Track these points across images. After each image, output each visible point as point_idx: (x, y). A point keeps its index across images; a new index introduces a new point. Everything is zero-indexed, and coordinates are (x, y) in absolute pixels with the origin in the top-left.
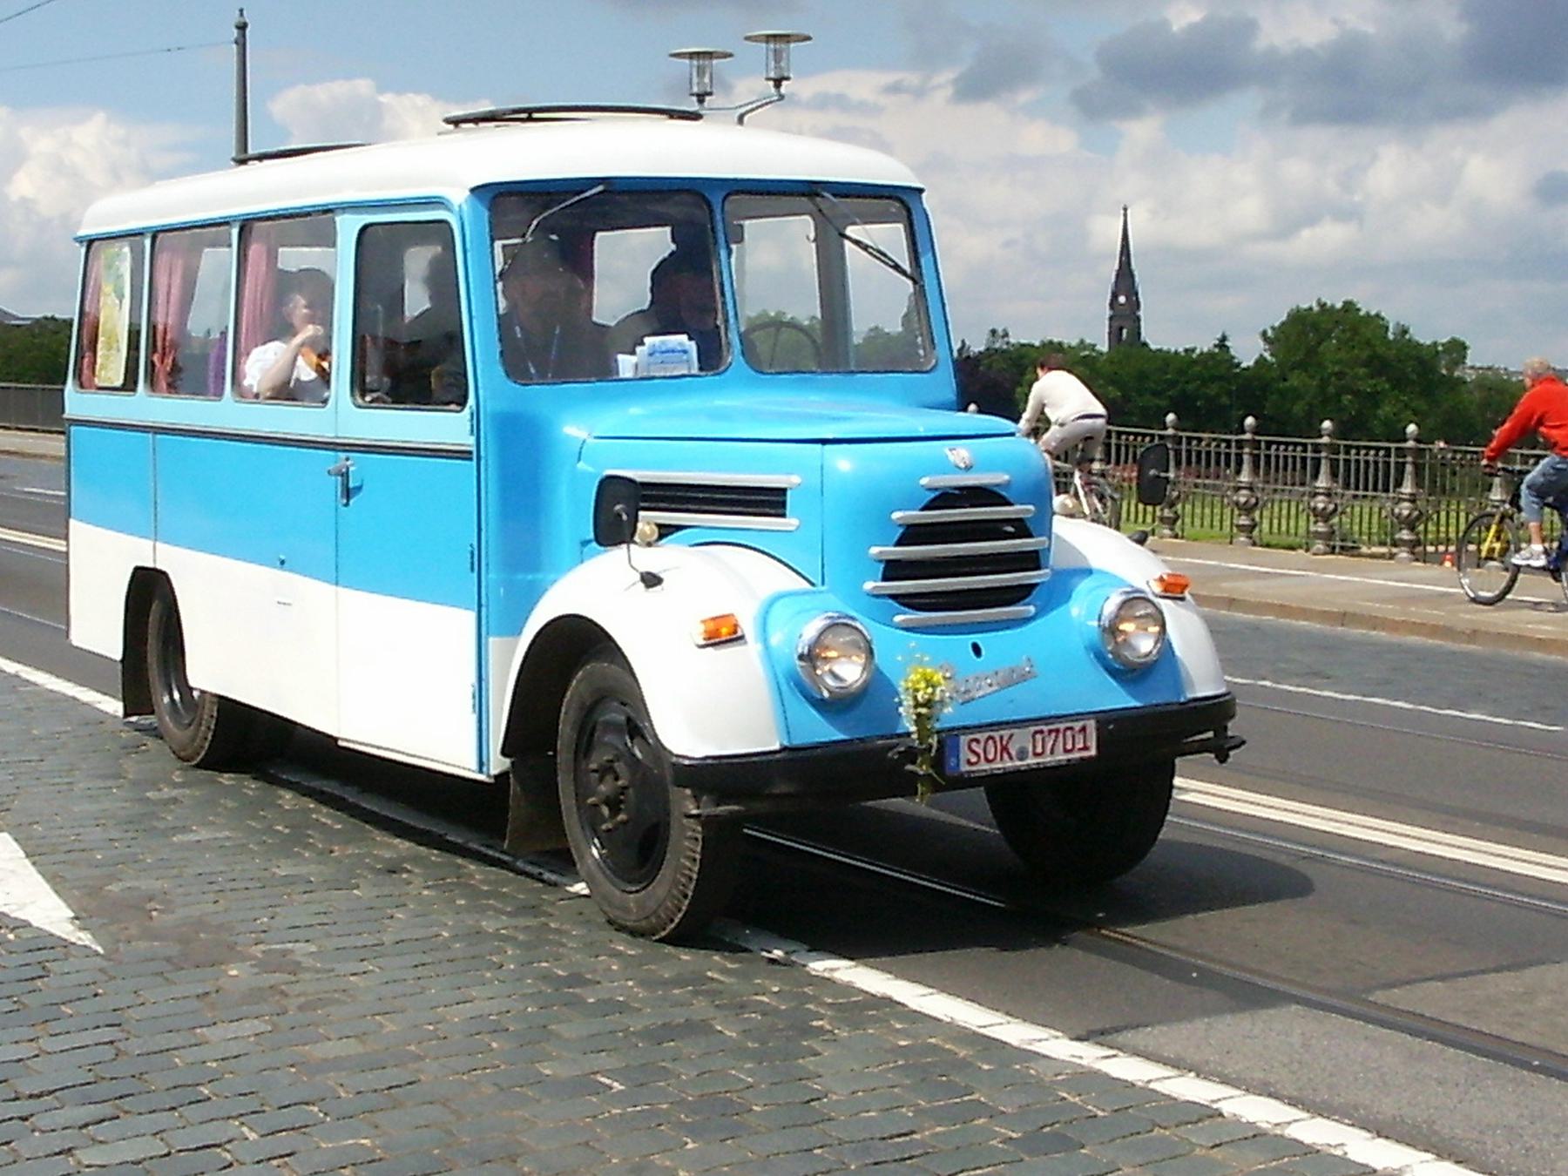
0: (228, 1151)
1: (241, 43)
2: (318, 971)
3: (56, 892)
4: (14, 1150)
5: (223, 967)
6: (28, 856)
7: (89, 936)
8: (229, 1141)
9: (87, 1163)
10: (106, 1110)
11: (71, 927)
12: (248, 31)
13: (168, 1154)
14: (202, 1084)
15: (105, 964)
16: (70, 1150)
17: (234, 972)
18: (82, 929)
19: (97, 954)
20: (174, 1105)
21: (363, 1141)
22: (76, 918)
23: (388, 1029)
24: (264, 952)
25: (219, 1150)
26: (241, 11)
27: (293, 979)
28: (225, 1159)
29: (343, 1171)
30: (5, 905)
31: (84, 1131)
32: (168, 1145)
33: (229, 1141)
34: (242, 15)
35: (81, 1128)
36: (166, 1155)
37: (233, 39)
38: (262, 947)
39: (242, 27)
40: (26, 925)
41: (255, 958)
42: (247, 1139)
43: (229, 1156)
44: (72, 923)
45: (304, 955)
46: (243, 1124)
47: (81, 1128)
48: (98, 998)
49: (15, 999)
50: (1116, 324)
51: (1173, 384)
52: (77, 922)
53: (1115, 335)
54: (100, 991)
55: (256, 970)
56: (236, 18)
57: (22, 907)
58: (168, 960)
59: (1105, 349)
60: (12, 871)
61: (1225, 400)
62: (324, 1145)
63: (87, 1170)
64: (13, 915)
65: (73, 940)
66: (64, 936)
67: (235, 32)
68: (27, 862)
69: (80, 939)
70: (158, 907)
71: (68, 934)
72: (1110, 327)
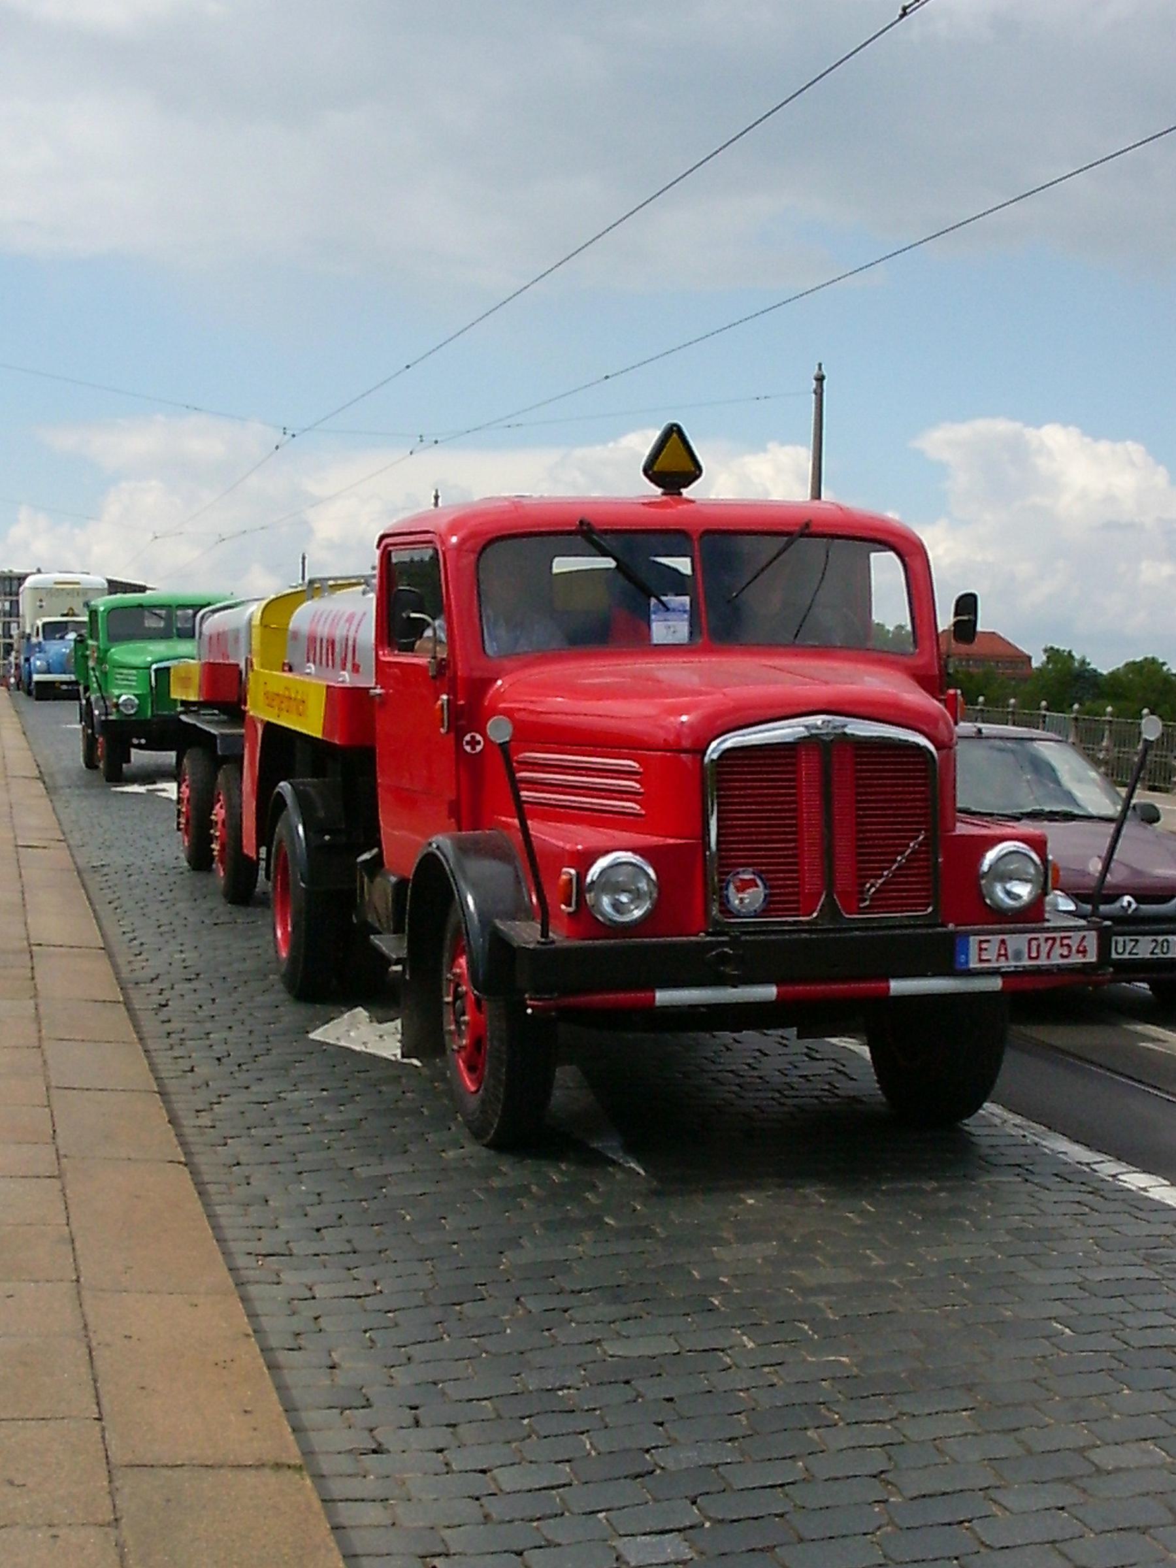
0: (728, 1355)
2: (821, 1205)
4: (553, 1336)
8: (731, 1348)
9: (611, 1353)
10: (634, 1309)
12: (825, 382)
13: (678, 1353)
14: (712, 1296)
16: (599, 1340)
17: (751, 1201)
20: (687, 1312)
21: (843, 1359)
23: (874, 1263)
26: (820, 365)
28: (726, 1363)
29: (823, 1383)
31: (612, 1325)
32: (681, 1346)
33: (731, 1348)
35: (610, 1323)
36: (674, 1354)
37: (812, 390)
39: (820, 379)
42: (745, 1346)
43: (728, 1360)
46: (743, 1334)
47: (610, 1323)
55: (770, 1201)
56: (816, 371)
62: (809, 1359)
63: (610, 1359)
67: (814, 382)
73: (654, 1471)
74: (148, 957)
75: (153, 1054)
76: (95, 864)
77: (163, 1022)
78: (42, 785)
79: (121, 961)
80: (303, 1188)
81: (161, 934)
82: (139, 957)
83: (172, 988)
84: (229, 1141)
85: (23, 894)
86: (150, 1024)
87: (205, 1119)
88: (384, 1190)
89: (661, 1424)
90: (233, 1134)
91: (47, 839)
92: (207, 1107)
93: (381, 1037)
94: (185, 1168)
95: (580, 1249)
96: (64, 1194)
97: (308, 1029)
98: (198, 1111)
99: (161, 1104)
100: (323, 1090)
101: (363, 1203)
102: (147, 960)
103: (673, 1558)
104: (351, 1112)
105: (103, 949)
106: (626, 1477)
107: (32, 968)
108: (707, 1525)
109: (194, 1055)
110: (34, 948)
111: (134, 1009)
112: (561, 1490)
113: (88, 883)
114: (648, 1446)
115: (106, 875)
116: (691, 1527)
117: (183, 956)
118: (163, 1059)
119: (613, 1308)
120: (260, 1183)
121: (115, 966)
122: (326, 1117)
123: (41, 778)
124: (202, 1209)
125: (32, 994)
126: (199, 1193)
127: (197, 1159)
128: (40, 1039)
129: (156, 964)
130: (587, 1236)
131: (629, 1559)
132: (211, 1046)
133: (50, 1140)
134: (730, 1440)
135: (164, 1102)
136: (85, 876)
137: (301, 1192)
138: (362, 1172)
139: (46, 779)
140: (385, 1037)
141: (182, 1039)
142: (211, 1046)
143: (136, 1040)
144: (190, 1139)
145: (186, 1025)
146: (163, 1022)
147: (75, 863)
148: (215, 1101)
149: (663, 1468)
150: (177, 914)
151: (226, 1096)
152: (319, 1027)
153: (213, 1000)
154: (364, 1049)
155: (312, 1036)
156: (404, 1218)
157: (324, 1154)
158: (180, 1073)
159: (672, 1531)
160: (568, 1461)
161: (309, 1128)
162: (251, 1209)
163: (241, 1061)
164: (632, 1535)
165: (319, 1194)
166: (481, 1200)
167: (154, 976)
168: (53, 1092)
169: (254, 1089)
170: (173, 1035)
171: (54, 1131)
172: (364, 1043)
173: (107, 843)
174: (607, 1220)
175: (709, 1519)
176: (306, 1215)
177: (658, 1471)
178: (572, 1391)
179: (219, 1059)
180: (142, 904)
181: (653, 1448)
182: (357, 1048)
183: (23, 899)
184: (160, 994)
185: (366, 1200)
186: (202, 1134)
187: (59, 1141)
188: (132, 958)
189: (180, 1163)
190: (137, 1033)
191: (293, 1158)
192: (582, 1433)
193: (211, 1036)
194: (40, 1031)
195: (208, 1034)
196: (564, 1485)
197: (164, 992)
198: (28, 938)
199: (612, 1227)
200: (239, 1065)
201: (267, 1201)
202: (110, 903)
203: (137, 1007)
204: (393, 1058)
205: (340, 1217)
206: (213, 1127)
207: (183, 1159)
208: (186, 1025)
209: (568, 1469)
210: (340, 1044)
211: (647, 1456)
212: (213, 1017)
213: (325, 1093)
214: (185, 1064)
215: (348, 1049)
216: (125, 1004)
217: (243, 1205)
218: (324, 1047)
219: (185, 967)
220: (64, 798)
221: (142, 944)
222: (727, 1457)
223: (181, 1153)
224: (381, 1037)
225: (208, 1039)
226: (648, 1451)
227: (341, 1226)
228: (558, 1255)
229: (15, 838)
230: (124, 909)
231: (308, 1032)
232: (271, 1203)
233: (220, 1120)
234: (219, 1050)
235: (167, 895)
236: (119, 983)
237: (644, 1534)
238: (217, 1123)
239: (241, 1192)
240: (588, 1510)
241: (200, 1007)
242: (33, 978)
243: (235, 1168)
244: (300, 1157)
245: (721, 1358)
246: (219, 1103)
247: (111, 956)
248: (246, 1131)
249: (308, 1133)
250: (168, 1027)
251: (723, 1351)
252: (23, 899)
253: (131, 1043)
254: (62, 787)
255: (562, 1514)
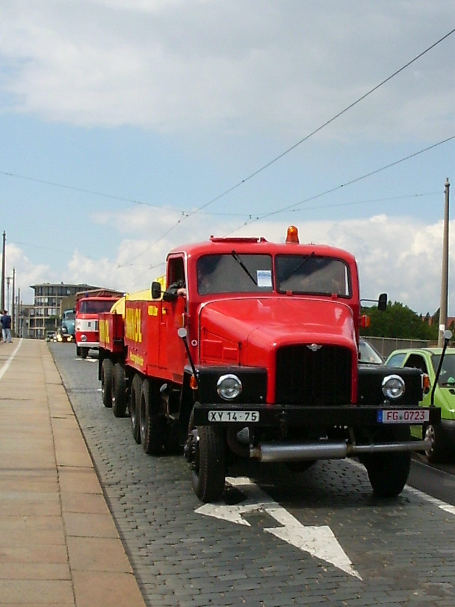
1: (447, 193)
3: (346, 553)
5: (412, 591)
6: (336, 536)
7: (357, 573)
11: (350, 568)
12: (450, 187)
15: (362, 585)
17: (416, 594)
18: (354, 569)
19: (360, 580)
22: (353, 564)
24: (429, 586)
26: (448, 179)
27: (441, 598)
30: (325, 556)
34: (447, 181)
38: (430, 584)
39: (448, 186)
40: (332, 565)
41: (426, 588)
44: (351, 567)
45: (447, 589)
48: (358, 599)
49: (324, 597)
52: (353, 566)
54: (360, 597)
55: (425, 594)
57: (331, 558)
58: (389, 586)
60: (329, 542)
64: (327, 561)
65: (351, 574)
66: (347, 572)
68: (335, 539)
69: (354, 574)
70: (387, 562)
71: (348, 571)
74: (115, 472)
75: (118, 520)
76: (88, 426)
77: (122, 504)
78: (63, 388)
79: (101, 474)
80: (192, 586)
81: (122, 461)
82: (111, 472)
83: (127, 487)
84: (155, 563)
85: (53, 440)
86: (115, 504)
87: (143, 552)
88: (232, 587)
90: (157, 559)
91: (67, 414)
92: (144, 546)
93: (230, 511)
94: (134, 577)
96: (73, 589)
97: (195, 508)
98: (140, 548)
99: (122, 545)
100: (201, 538)
101: (222, 594)
102: (114, 474)
104: (217, 549)
105: (92, 467)
107: (58, 477)
109: (138, 520)
110: (59, 468)
111: (108, 498)
113: (86, 436)
115: (94, 432)
117: (132, 471)
118: (122, 523)
120: (171, 582)
121: (99, 476)
122: (203, 551)
123: (62, 384)
124: (141, 596)
125: (58, 489)
126: (140, 589)
127: (139, 572)
128: (62, 512)
129: (118, 476)
132: (146, 516)
133: (66, 562)
135: (123, 543)
136: (84, 432)
137: (191, 588)
138: (222, 578)
139: (65, 385)
140: (233, 512)
141: (131, 513)
142: (146, 516)
143: (109, 512)
144: (135, 562)
145: (133, 506)
146: (122, 504)
147: (80, 426)
148: (148, 543)
150: (129, 451)
151: (154, 541)
152: (199, 507)
153: (147, 493)
154: (222, 518)
155: (196, 511)
156: (242, 601)
157: (202, 570)
158: (130, 530)
161: (194, 557)
162: (165, 597)
163: (161, 523)
165: (200, 589)
166: (280, 593)
167: (118, 481)
168: (68, 538)
169: (167, 537)
170: (127, 511)
171: (68, 557)
172: (223, 515)
173: (95, 416)
176: (193, 600)
179: (150, 523)
180: (111, 446)
182: (219, 517)
183: (54, 443)
184: (121, 490)
185: (222, 592)
186: (142, 559)
187: (70, 562)
188: (107, 472)
189: (130, 573)
190: (110, 509)
191: (187, 571)
193: (146, 511)
194: (61, 508)
195: (145, 510)
197: (124, 489)
198: (56, 463)
200: (160, 525)
201: (174, 593)
202: (96, 445)
203: (109, 496)
204: (236, 522)
205: (210, 601)
206: (147, 556)
207: (132, 572)
208: (133, 506)
210: (210, 515)
212: (147, 502)
213: (203, 539)
214: (133, 525)
215: (213, 517)
216: (104, 495)
217: (162, 594)
218: (203, 517)
219: (133, 477)
220: (74, 394)
221: (112, 466)
223: (132, 569)
224: (230, 511)
225: (145, 512)
227: (211, 605)
229: (50, 414)
230: (103, 448)
231: (194, 509)
232: (176, 593)
233: (152, 553)
234: (150, 518)
235: (124, 442)
236: (101, 485)
238: (149, 554)
239: (161, 588)
241: (141, 497)
242: (58, 482)
243: (158, 576)
244: (190, 571)
246: (150, 544)
247: (97, 472)
248: (163, 558)
249: (195, 559)
250: (124, 507)
252: (54, 443)
253: (107, 514)
254: (72, 389)
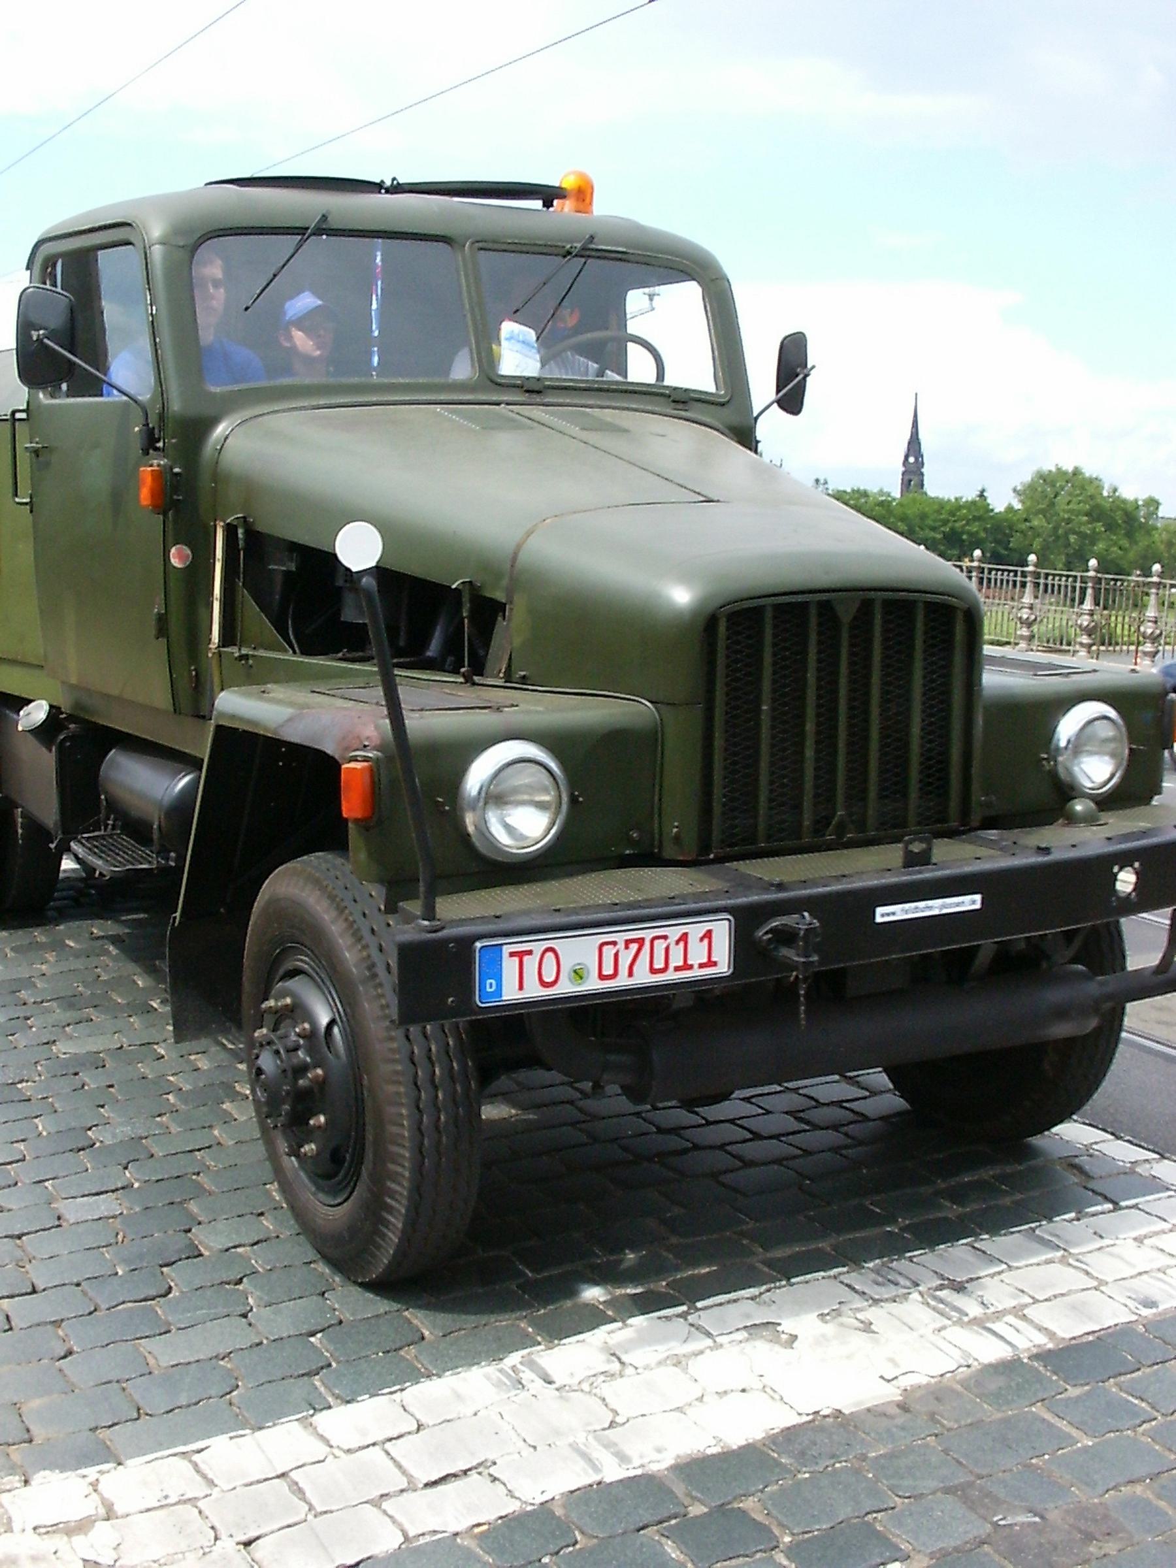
13: (122, 1047)
16: (55, 1041)
25: (156, 1047)
28: (159, 1054)
31: (67, 1029)
50: (907, 478)
51: (945, 522)
53: (906, 484)
59: (898, 495)
61: (983, 535)
63: (64, 1056)
72: (902, 479)
73: (94, 1144)
89: (102, 1106)
95: (44, 967)
103: (106, 1214)
106: (71, 1151)
108: (136, 1185)
112: (14, 1165)
114: (90, 1125)
116: (123, 1188)
119: (68, 1014)
130: (51, 957)
131: (68, 1217)
134: (159, 1115)
149: (102, 1142)
159: (107, 1192)
160: (23, 1141)
164: (72, 1198)
174: (67, 942)
175: (137, 1180)
177: (98, 1144)
178: (29, 1084)
181: (96, 1126)
192: (36, 1117)
196: (17, 1161)
199: (71, 947)
209: (22, 1148)
211: (89, 1133)
222: (155, 1129)
226: (90, 1129)
228: (23, 972)
237: (83, 1196)
240: (37, 1179)
245: (155, 1050)
251: (157, 1044)
255: (16, 1184)
